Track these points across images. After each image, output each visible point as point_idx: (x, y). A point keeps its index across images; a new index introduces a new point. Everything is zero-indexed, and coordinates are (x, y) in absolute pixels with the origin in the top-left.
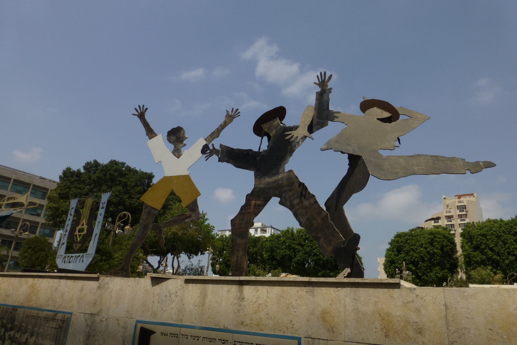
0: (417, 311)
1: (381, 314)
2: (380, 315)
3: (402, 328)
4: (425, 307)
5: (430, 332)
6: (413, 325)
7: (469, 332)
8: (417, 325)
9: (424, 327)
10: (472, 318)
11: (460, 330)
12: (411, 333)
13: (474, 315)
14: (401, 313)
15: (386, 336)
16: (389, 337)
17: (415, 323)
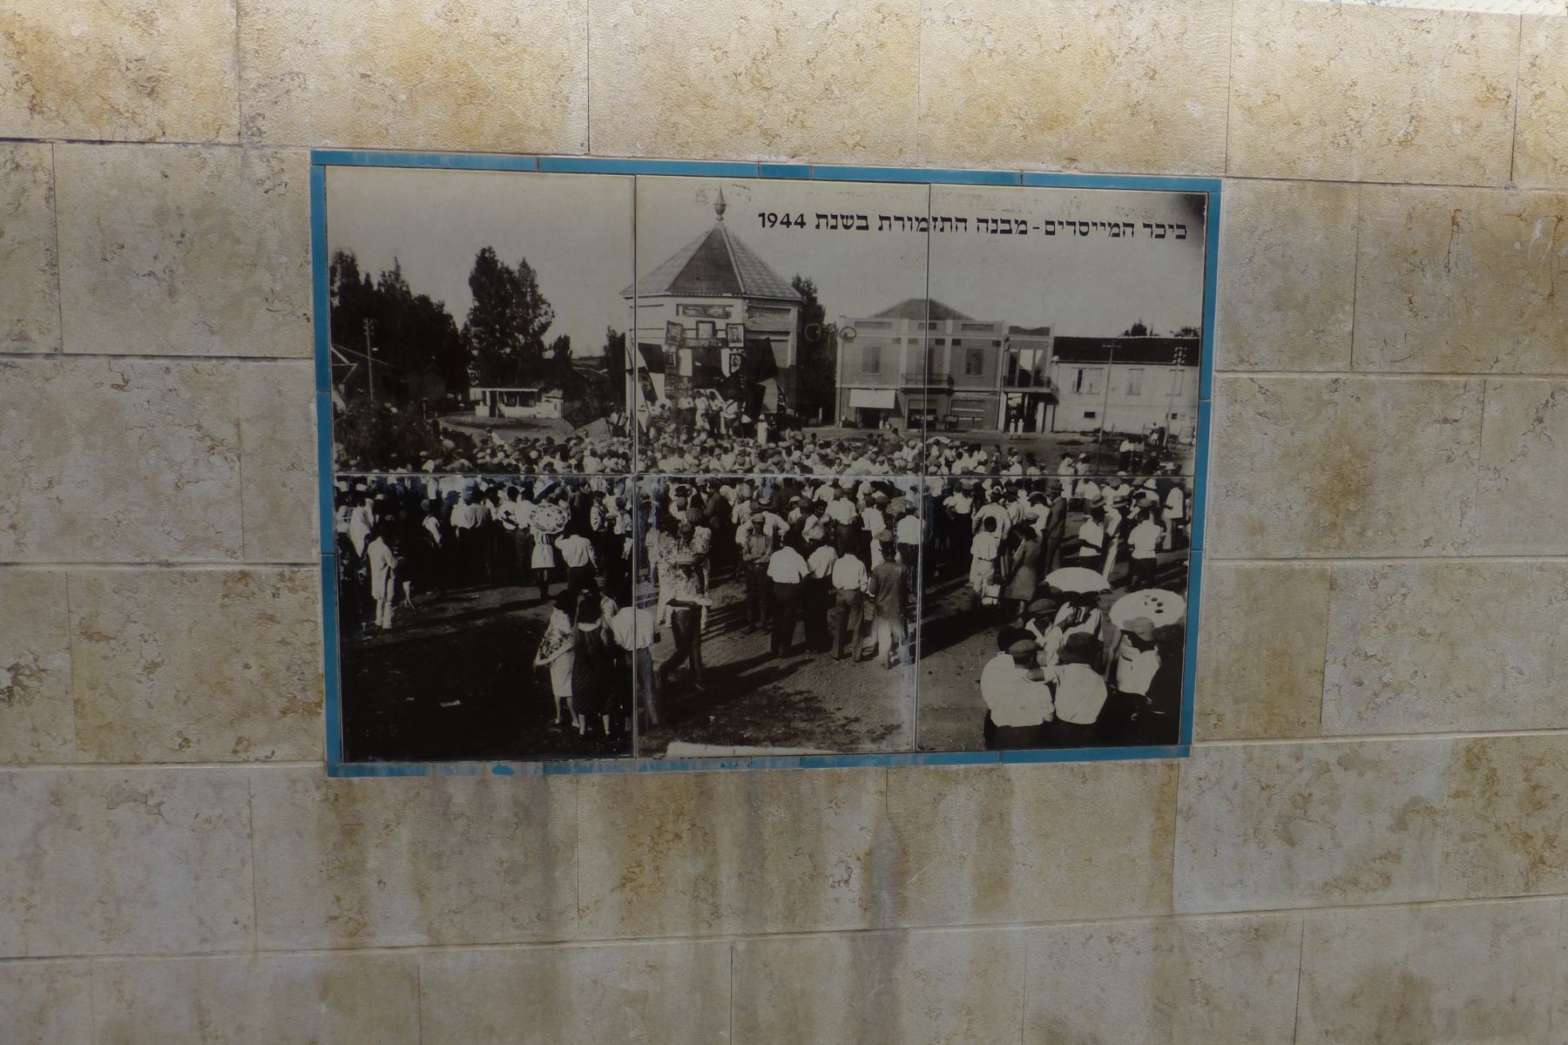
0: (141, 23)
1: (14, 33)
2: (10, 36)
3: (92, 80)
4: (169, 10)
5: (185, 90)
6: (128, 69)
7: (302, 86)
8: (140, 69)
9: (164, 74)
10: (316, 43)
11: (278, 81)
12: (121, 95)
13: (323, 32)
14: (86, 28)
15: (32, 109)
16: (45, 109)
17: (136, 60)
